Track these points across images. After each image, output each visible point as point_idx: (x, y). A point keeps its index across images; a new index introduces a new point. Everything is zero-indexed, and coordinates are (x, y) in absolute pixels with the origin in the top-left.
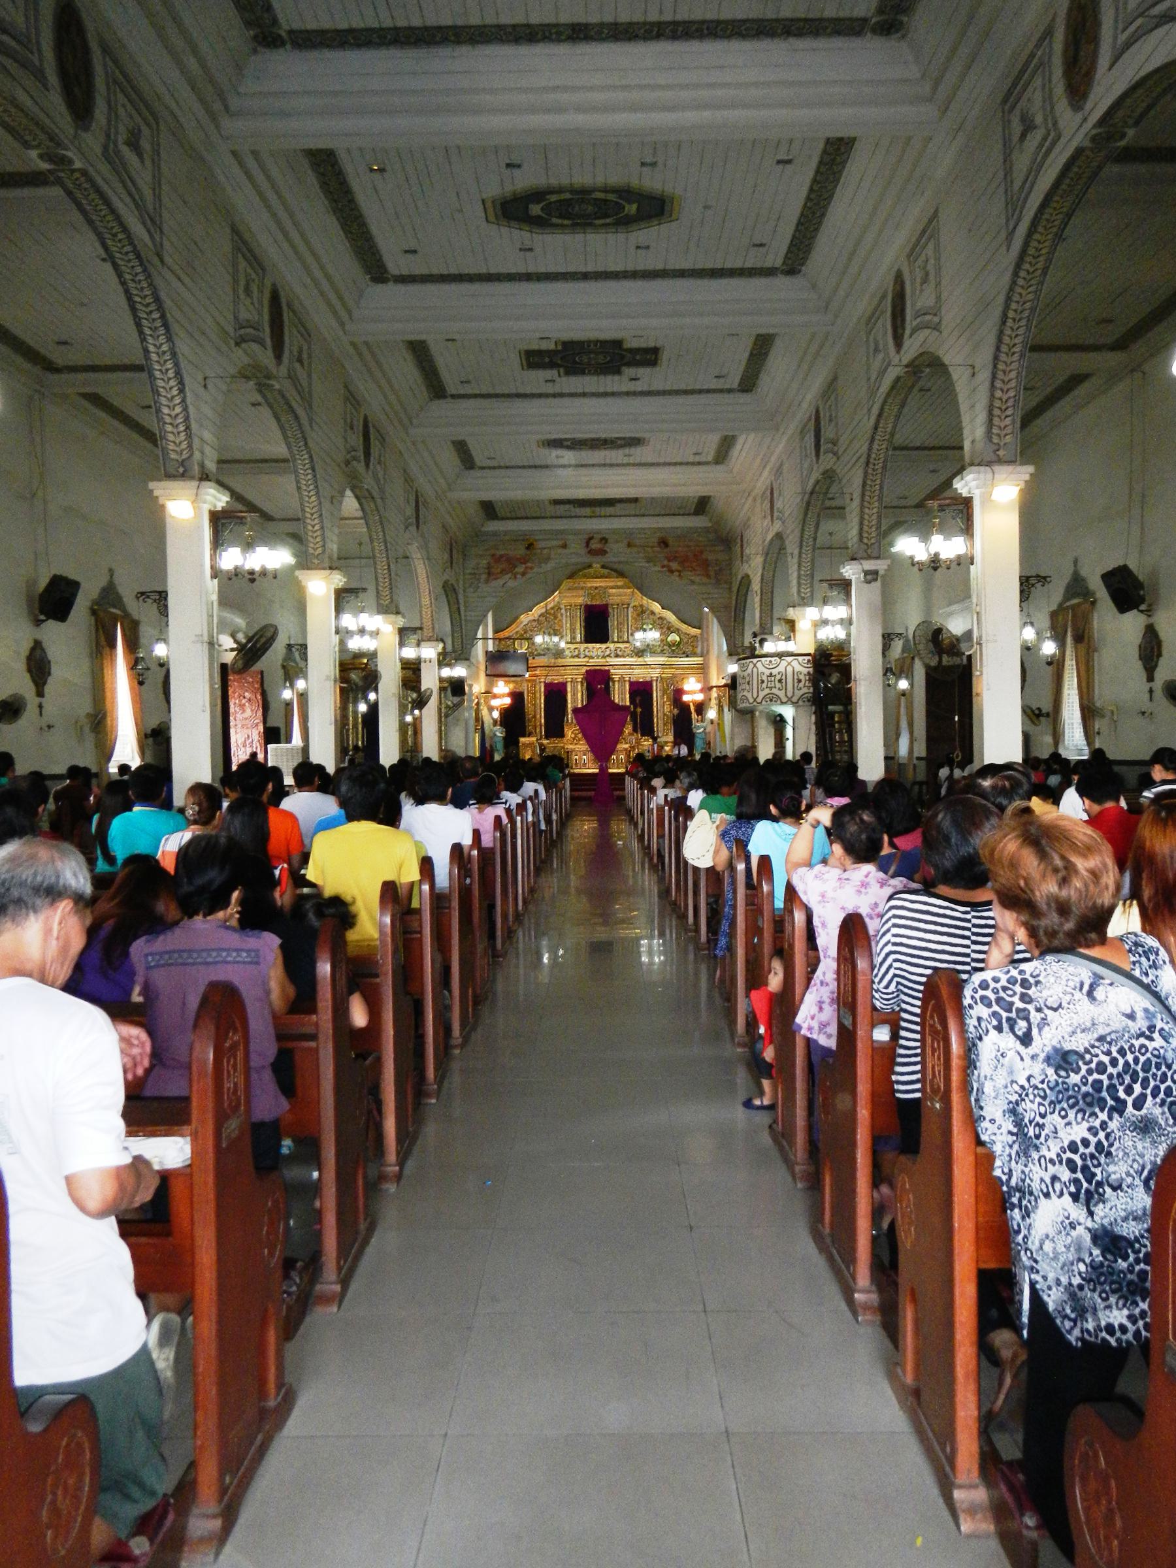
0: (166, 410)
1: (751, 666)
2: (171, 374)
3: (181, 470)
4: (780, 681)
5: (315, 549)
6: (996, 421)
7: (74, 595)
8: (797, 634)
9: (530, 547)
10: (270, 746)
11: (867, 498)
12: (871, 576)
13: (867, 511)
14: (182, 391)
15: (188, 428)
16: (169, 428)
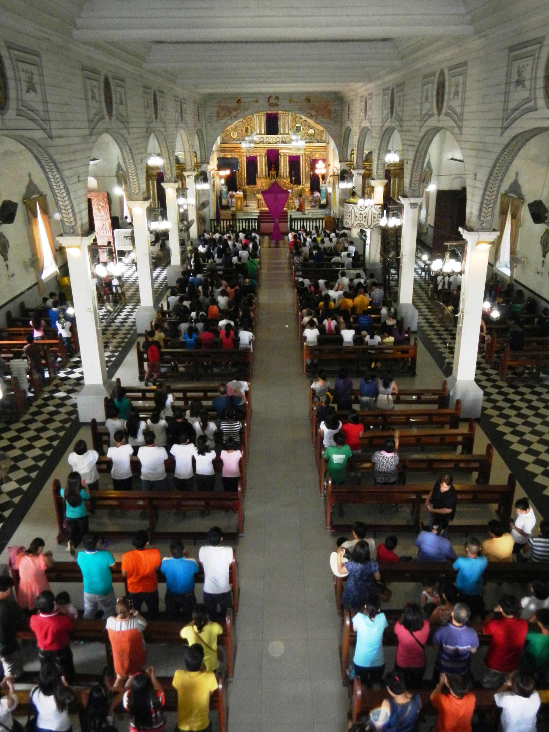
0: (61, 203)
1: (351, 208)
2: (62, 187)
3: (72, 231)
4: (365, 217)
5: (135, 191)
6: (484, 210)
7: (15, 210)
9: (239, 101)
10: (116, 231)
11: (415, 167)
12: (413, 205)
13: (415, 173)
14: (68, 194)
15: (73, 211)
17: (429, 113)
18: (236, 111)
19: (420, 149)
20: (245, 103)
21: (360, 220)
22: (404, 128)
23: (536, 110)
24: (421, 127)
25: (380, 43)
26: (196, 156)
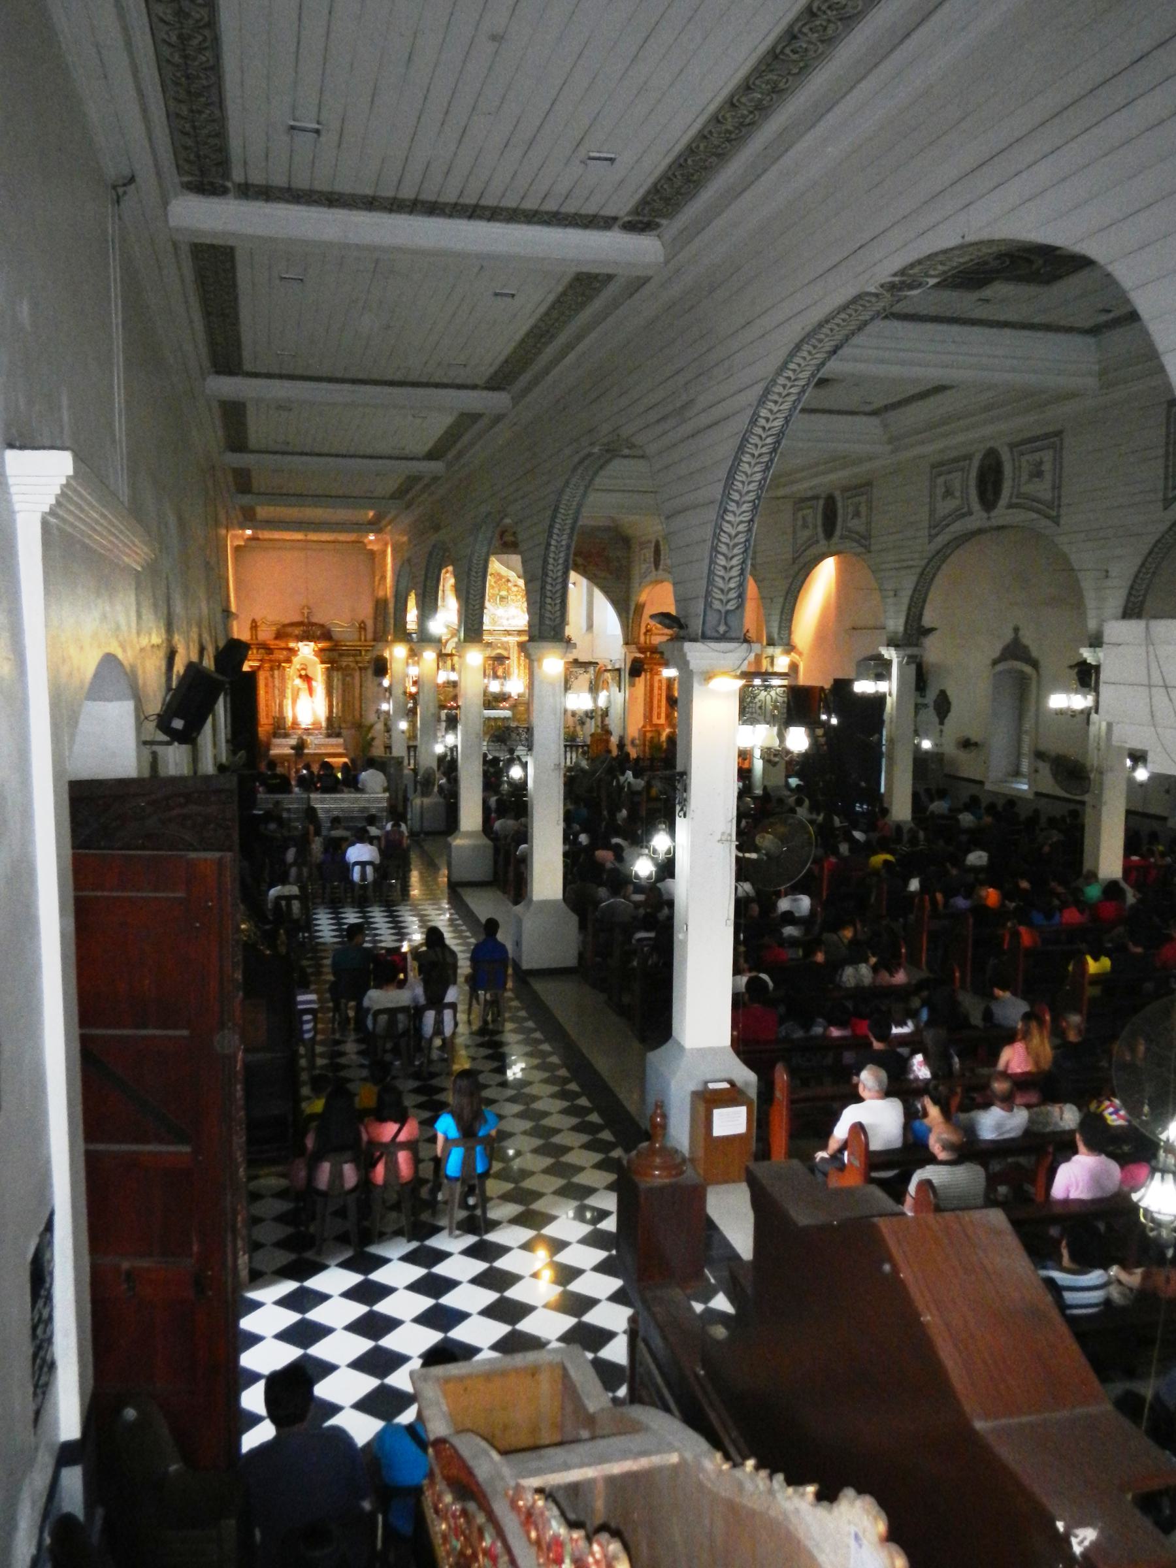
0: (549, 587)
2: (561, 561)
4: (760, 708)
16: (548, 600)
22: (873, 548)
24: (932, 537)
26: (365, 629)
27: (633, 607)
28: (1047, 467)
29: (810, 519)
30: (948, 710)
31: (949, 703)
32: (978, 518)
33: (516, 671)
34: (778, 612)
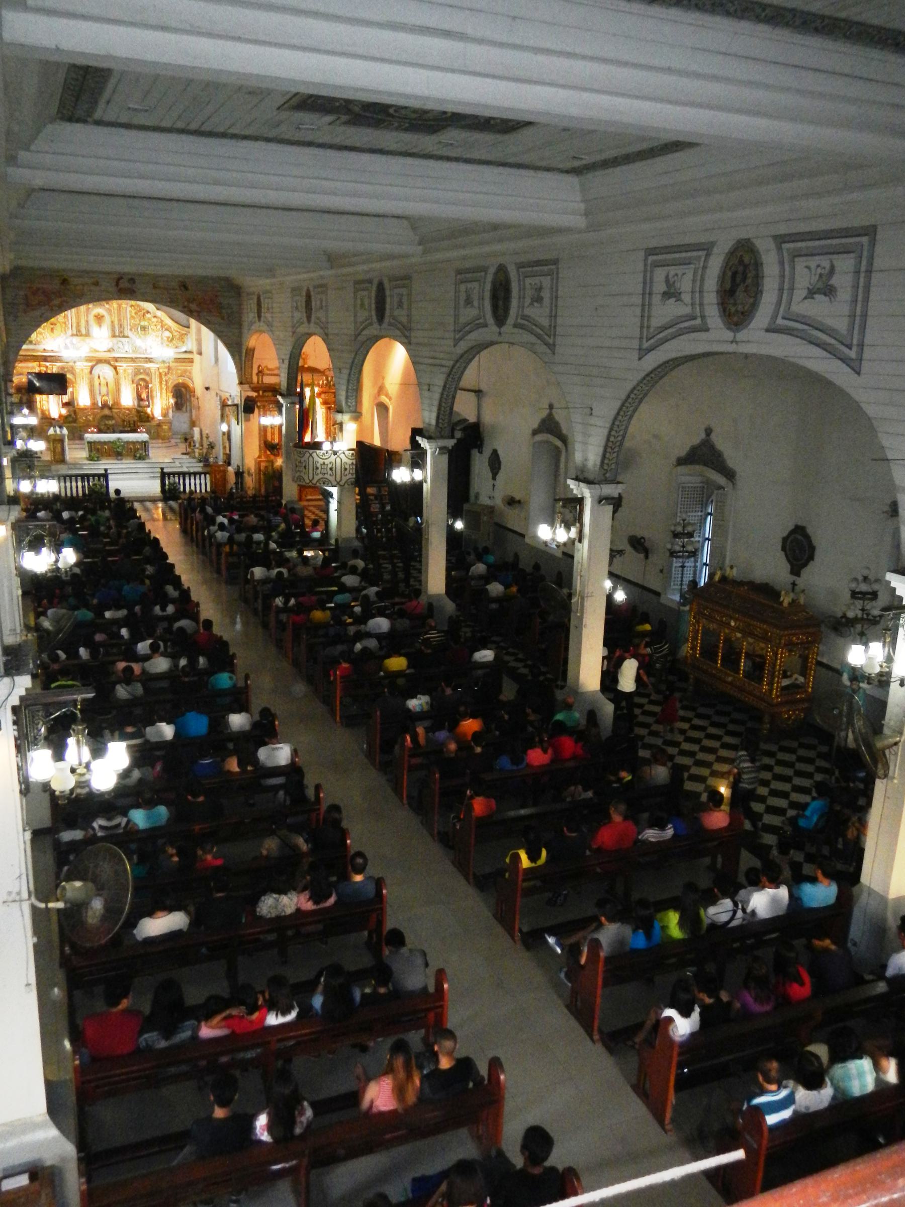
1: (307, 455)
4: (331, 469)
6: (608, 455)
8: (344, 432)
13: (443, 404)
17: (477, 322)
18: (61, 297)
19: (454, 370)
20: (75, 286)
21: (324, 474)
22: (414, 340)
23: (707, 330)
24: (456, 342)
25: (395, 221)
27: (244, 351)
28: (546, 294)
29: (366, 303)
30: (499, 468)
31: (499, 463)
32: (490, 331)
33: (159, 394)
34: (345, 382)
